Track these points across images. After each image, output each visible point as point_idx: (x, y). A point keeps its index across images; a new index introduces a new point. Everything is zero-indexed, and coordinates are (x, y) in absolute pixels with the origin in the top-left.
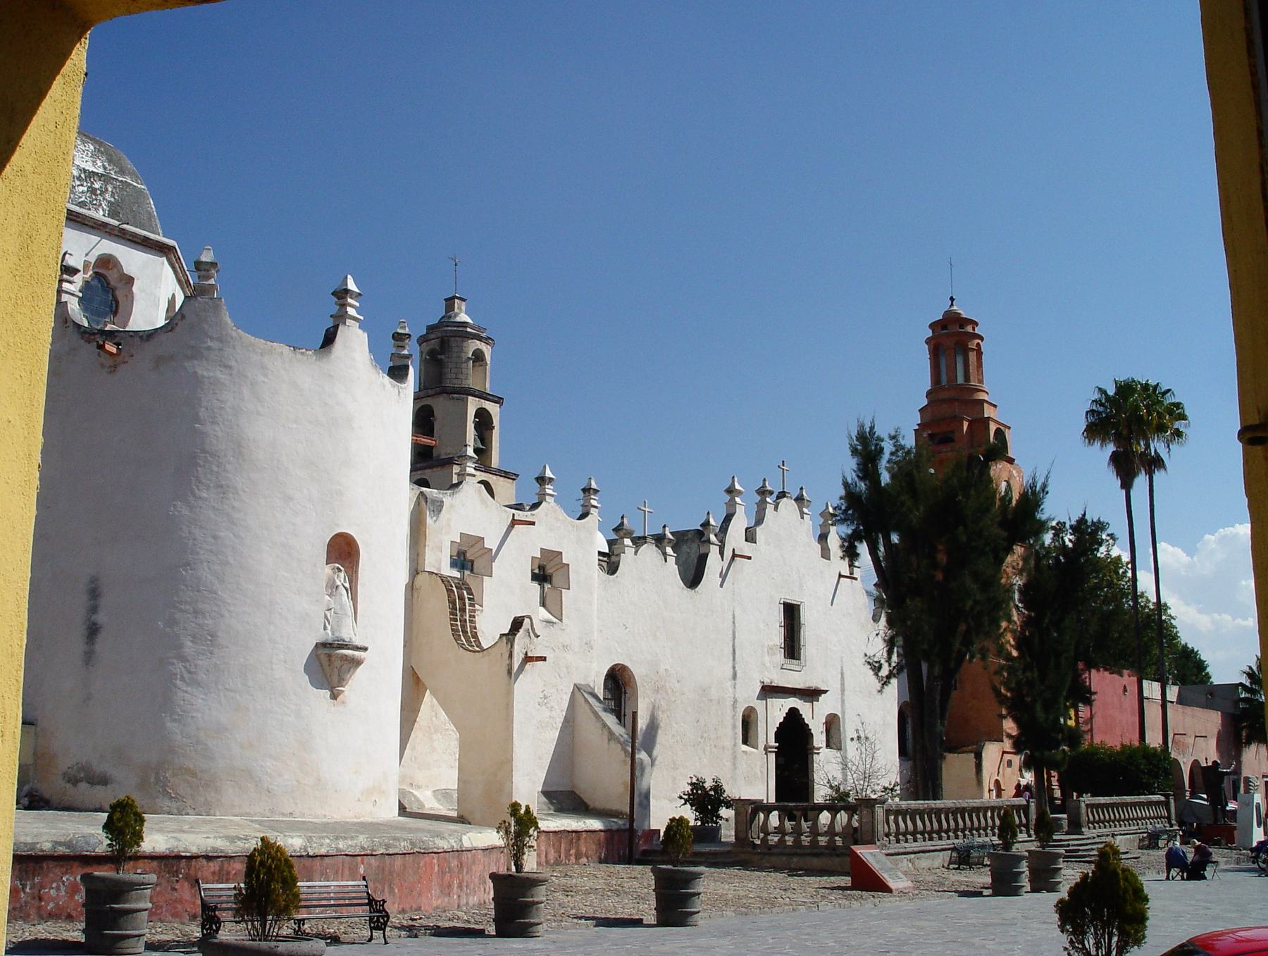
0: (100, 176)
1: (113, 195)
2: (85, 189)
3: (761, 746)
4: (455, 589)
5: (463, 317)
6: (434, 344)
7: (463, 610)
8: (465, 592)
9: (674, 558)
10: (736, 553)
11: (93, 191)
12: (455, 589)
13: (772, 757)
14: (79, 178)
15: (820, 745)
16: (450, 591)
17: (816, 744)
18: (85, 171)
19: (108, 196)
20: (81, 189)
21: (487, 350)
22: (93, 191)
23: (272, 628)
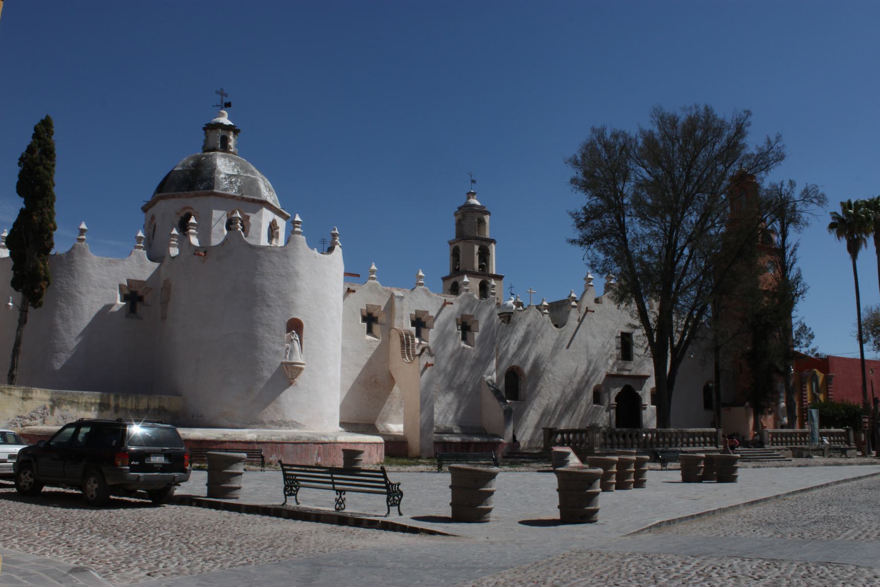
0: (234, 176)
1: (240, 183)
2: (227, 182)
3: (606, 403)
4: (404, 335)
5: (474, 201)
6: (460, 216)
7: (408, 345)
8: (410, 337)
9: (548, 315)
10: (589, 309)
11: (231, 182)
12: (404, 335)
13: (613, 411)
14: (225, 178)
15: (647, 403)
16: (401, 336)
17: (644, 403)
18: (228, 174)
19: (238, 184)
20: (226, 183)
21: (487, 218)
22: (231, 182)
23: (262, 357)
